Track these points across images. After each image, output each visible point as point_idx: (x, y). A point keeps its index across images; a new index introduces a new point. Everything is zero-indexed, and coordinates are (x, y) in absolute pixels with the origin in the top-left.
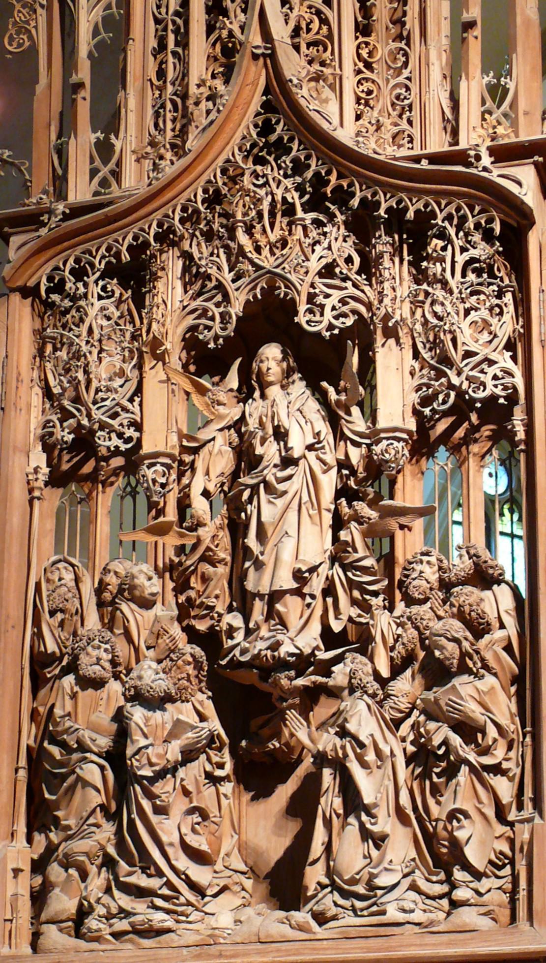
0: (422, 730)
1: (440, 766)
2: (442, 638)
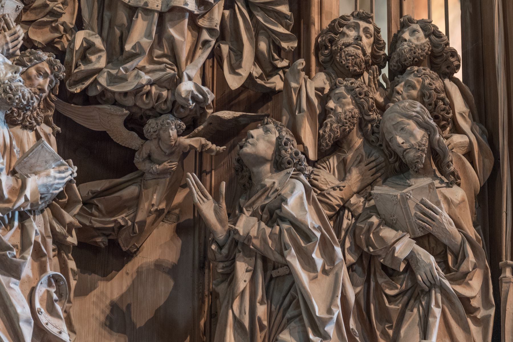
0: (371, 235)
1: (397, 288)
2: (411, 122)
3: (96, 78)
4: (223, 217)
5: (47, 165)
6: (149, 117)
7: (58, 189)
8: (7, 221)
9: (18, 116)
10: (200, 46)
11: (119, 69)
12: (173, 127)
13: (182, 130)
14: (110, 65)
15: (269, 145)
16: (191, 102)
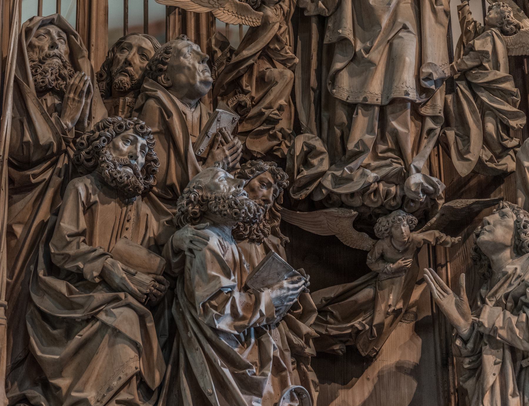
3: (320, 182)
4: (466, 311)
5: (280, 277)
6: (378, 216)
7: (292, 300)
8: (243, 339)
9: (244, 230)
10: (425, 135)
11: (344, 170)
12: (405, 222)
13: (414, 225)
14: (333, 166)
15: (507, 230)
16: (421, 195)
